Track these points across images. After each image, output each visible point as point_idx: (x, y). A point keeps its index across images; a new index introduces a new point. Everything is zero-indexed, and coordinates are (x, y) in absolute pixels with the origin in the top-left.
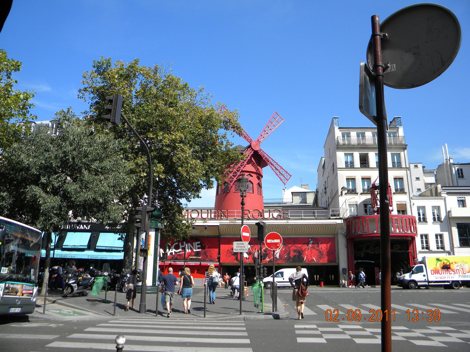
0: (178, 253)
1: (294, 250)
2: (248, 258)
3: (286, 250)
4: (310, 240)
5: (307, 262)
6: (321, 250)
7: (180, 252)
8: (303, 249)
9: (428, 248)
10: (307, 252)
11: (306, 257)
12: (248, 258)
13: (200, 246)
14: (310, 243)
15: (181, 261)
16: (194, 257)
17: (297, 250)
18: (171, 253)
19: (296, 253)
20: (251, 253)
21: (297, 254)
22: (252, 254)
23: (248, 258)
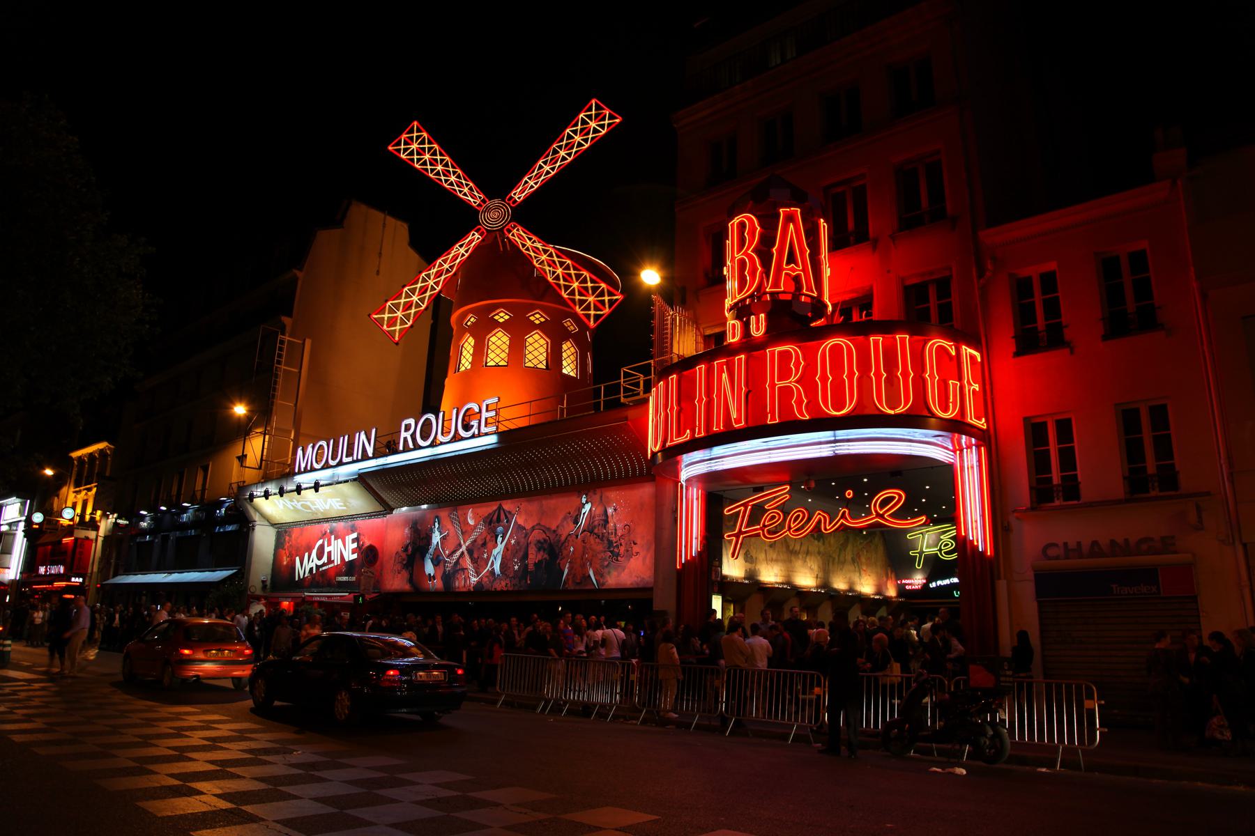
0: (321, 569)
1: (539, 541)
2: (432, 575)
3: (518, 543)
4: (584, 500)
5: (571, 587)
6: (612, 538)
7: (324, 565)
8: (563, 538)
9: (1071, 489)
10: (572, 549)
11: (567, 566)
12: (434, 577)
13: (355, 545)
14: (583, 511)
15: (324, 590)
16: (345, 579)
17: (545, 540)
18: (311, 569)
19: (541, 552)
20: (441, 558)
21: (544, 557)
22: (442, 564)
23: (432, 575)
